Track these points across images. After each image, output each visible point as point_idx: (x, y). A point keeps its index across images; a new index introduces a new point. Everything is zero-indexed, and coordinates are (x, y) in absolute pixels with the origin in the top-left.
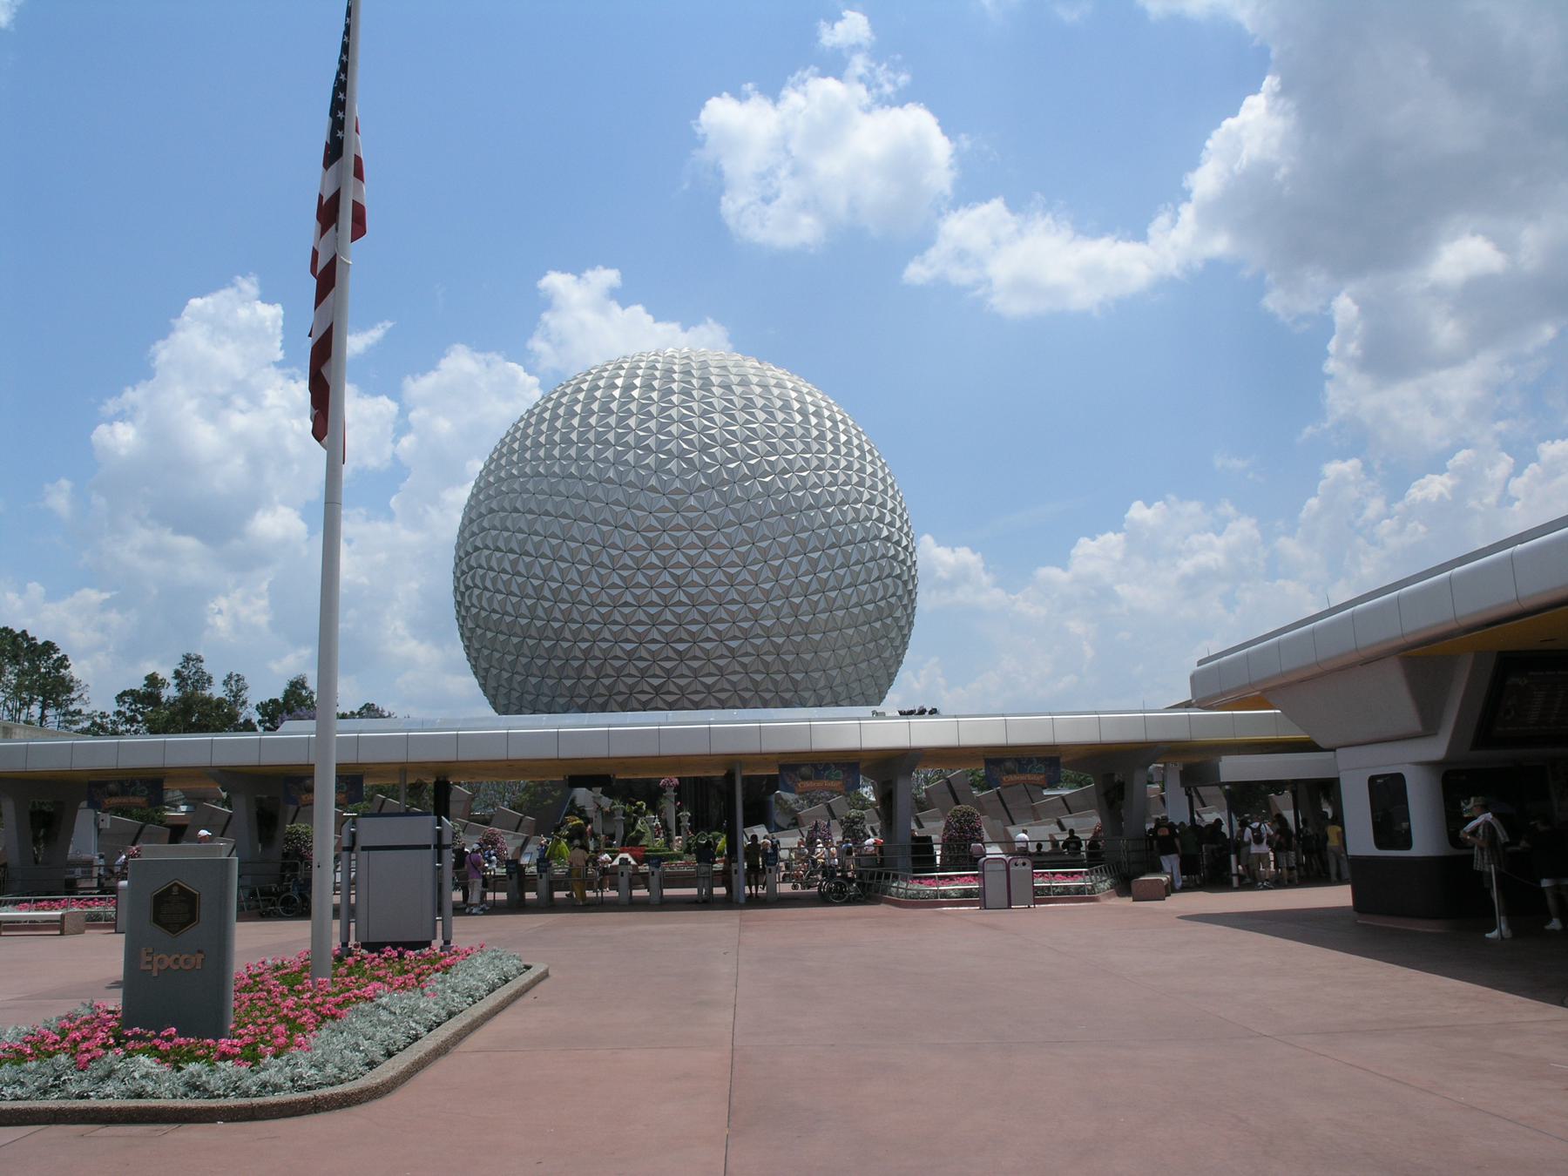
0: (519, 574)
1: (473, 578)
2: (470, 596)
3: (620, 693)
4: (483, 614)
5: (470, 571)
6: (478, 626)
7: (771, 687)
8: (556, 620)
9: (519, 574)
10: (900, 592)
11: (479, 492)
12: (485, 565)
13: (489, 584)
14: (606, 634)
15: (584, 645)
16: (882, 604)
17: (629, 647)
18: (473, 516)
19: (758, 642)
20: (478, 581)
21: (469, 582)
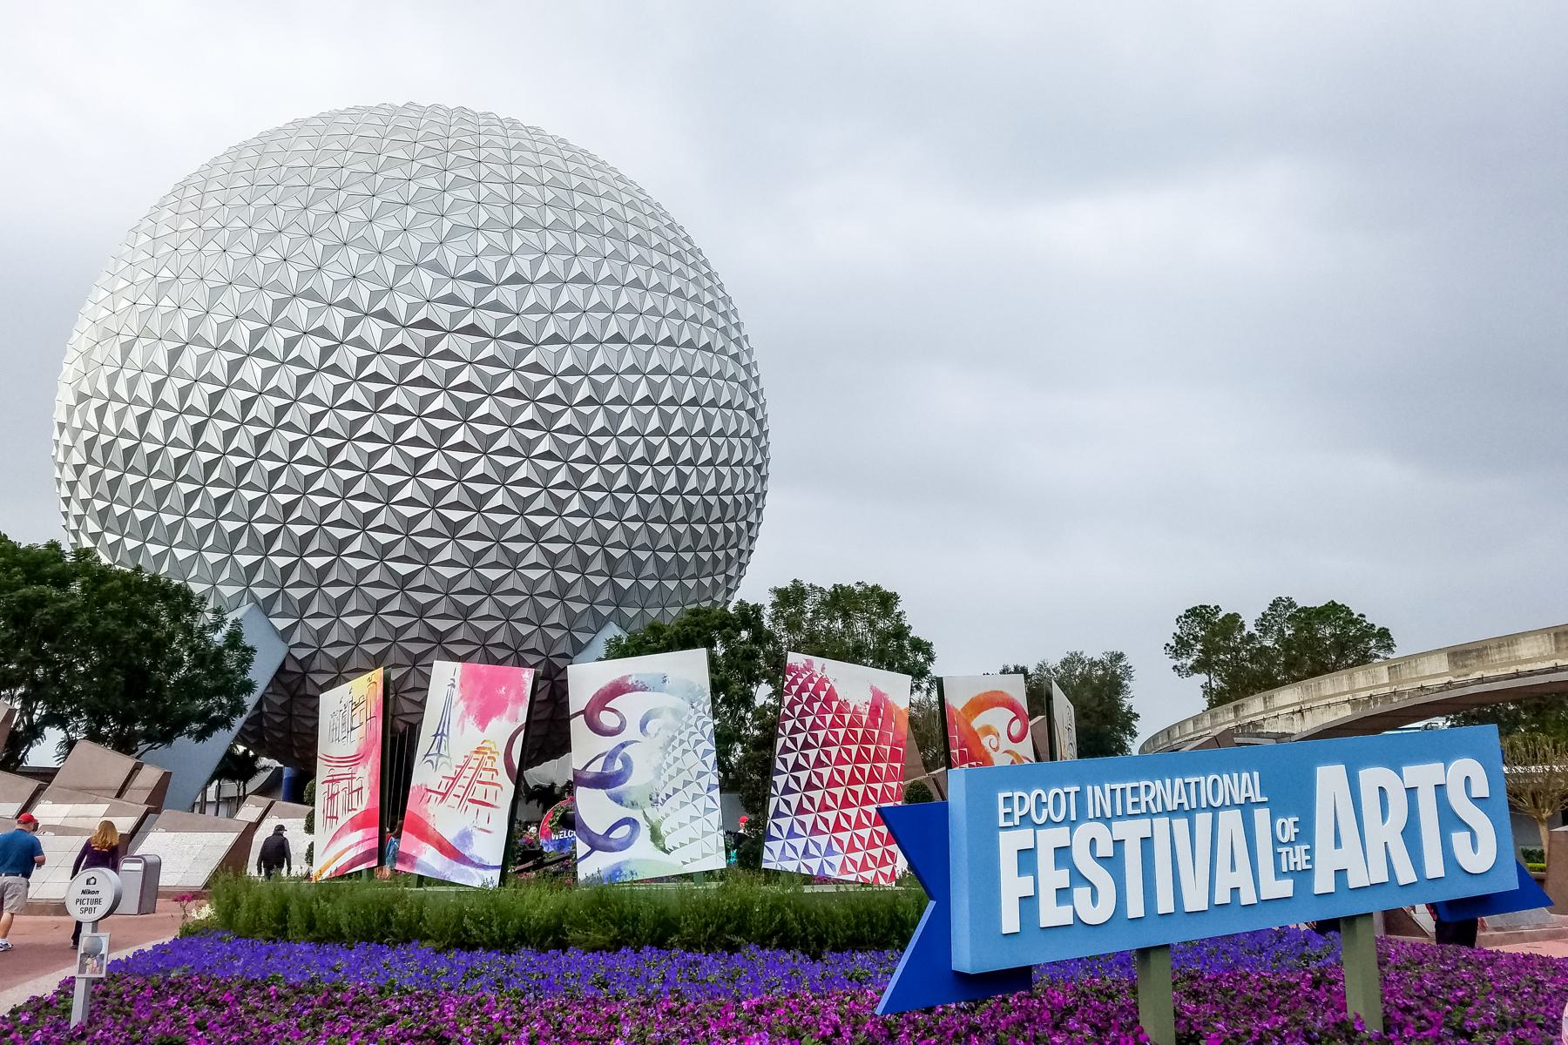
2: (83, 414)
6: (91, 461)
10: (758, 490)
13: (121, 389)
16: (741, 498)
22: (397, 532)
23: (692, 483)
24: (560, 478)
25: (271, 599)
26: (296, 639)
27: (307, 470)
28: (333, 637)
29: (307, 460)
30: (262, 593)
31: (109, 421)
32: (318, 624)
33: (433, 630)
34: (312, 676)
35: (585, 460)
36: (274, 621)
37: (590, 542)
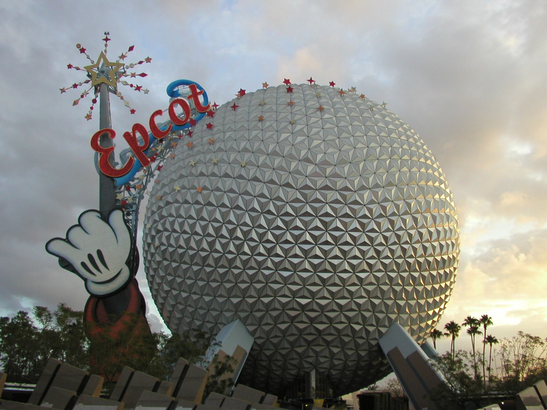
0: (203, 219)
1: (164, 224)
2: (160, 239)
3: (275, 309)
4: (171, 249)
5: (160, 220)
7: (384, 310)
8: (230, 252)
9: (203, 219)
11: (151, 206)
12: (174, 214)
13: (177, 227)
14: (269, 264)
15: (251, 272)
17: (286, 274)
18: (154, 208)
19: (379, 275)
20: (168, 226)
21: (160, 227)
22: (301, 285)
23: (430, 251)
24: (369, 255)
25: (247, 317)
26: (257, 335)
27: (260, 259)
28: (273, 335)
29: (260, 254)
30: (243, 315)
31: (172, 242)
32: (267, 328)
33: (317, 329)
34: (263, 351)
35: (381, 244)
36: (248, 327)
37: (385, 284)
